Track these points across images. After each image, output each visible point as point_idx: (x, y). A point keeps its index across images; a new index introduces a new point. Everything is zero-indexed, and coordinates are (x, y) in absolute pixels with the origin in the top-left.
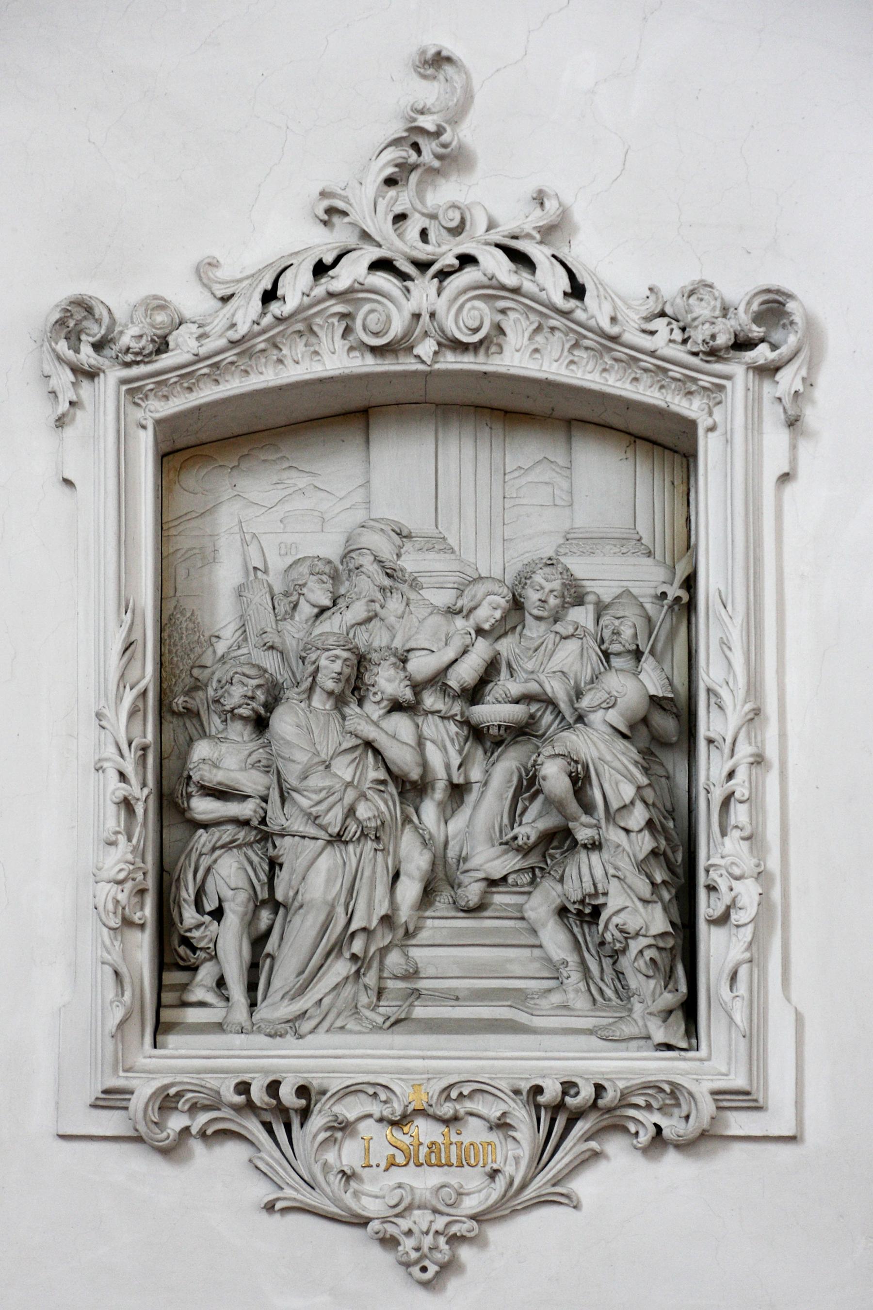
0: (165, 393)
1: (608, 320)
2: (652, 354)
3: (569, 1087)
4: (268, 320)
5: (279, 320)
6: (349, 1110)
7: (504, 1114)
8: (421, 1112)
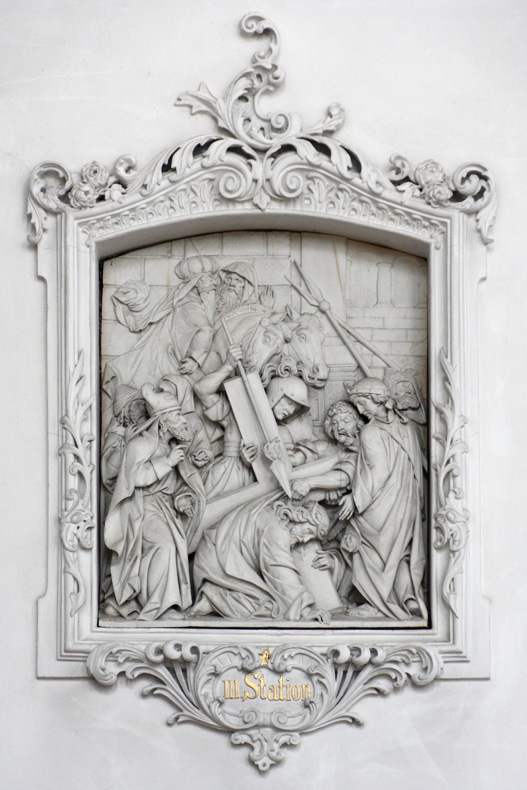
0: (102, 226)
2: (401, 204)
5: (173, 182)
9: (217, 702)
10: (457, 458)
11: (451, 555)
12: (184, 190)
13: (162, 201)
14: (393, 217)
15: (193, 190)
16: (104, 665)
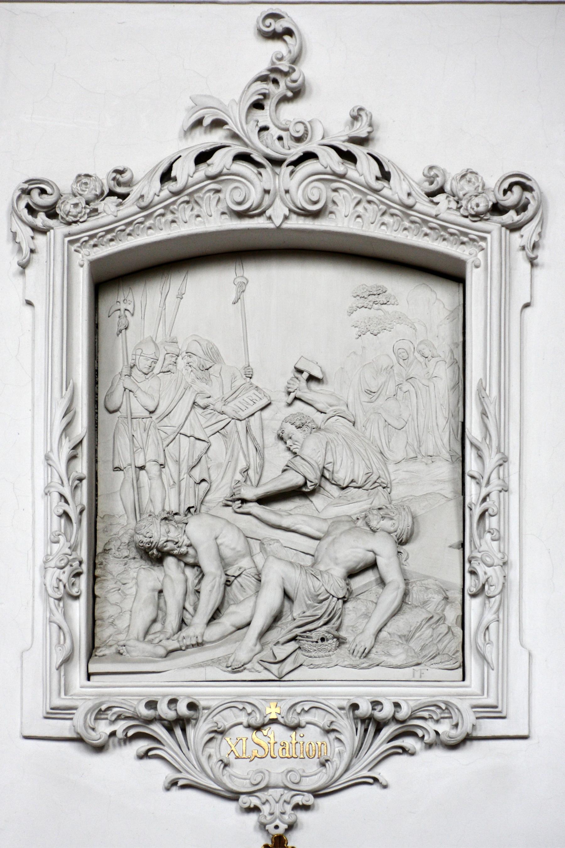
1: (406, 195)
3: (376, 704)
4: (165, 193)
6: (226, 719)
7: (332, 723)
8: (274, 721)
9: (220, 762)
10: (494, 496)
11: (487, 602)
12: (188, 202)
13: (163, 215)
14: (428, 231)
15: (197, 202)
16: (93, 724)
